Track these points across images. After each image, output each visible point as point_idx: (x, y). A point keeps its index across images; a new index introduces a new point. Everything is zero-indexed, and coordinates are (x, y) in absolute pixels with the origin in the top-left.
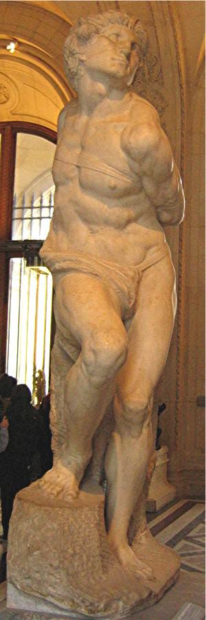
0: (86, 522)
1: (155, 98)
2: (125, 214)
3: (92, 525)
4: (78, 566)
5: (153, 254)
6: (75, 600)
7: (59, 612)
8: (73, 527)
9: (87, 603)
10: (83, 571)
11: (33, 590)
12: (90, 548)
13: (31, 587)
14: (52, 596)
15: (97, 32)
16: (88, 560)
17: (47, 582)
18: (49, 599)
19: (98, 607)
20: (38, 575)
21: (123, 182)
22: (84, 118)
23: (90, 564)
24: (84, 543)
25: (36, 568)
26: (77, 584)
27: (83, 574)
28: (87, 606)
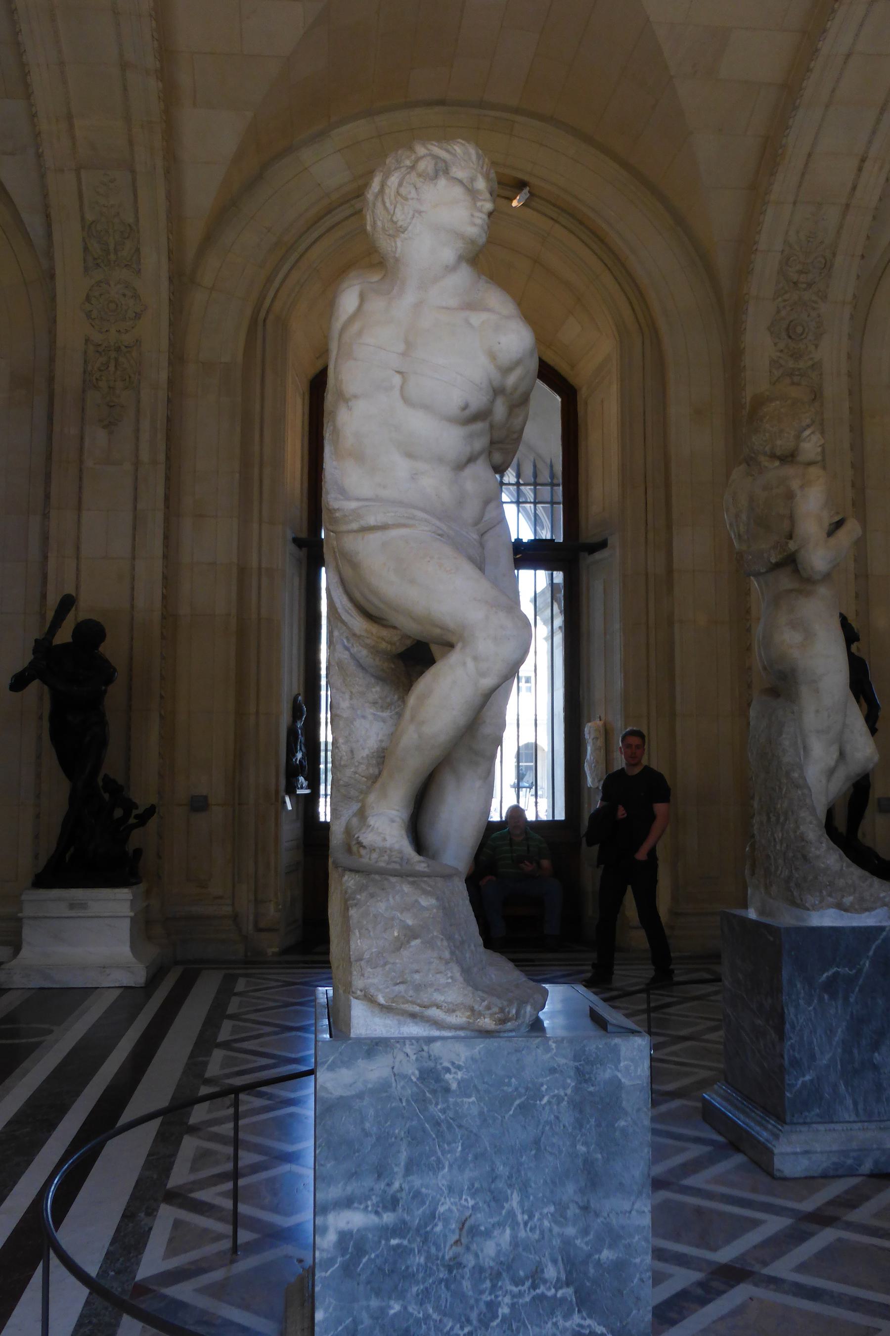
1: (124, 295)
6: (476, 1007)
7: (436, 1033)
9: (495, 1009)
11: (407, 1002)
13: (403, 997)
14: (438, 1007)
15: (446, 171)
17: (431, 985)
18: (434, 1012)
19: (509, 1012)
20: (417, 977)
21: (478, 401)
22: (409, 298)
25: (415, 967)
28: (491, 1015)
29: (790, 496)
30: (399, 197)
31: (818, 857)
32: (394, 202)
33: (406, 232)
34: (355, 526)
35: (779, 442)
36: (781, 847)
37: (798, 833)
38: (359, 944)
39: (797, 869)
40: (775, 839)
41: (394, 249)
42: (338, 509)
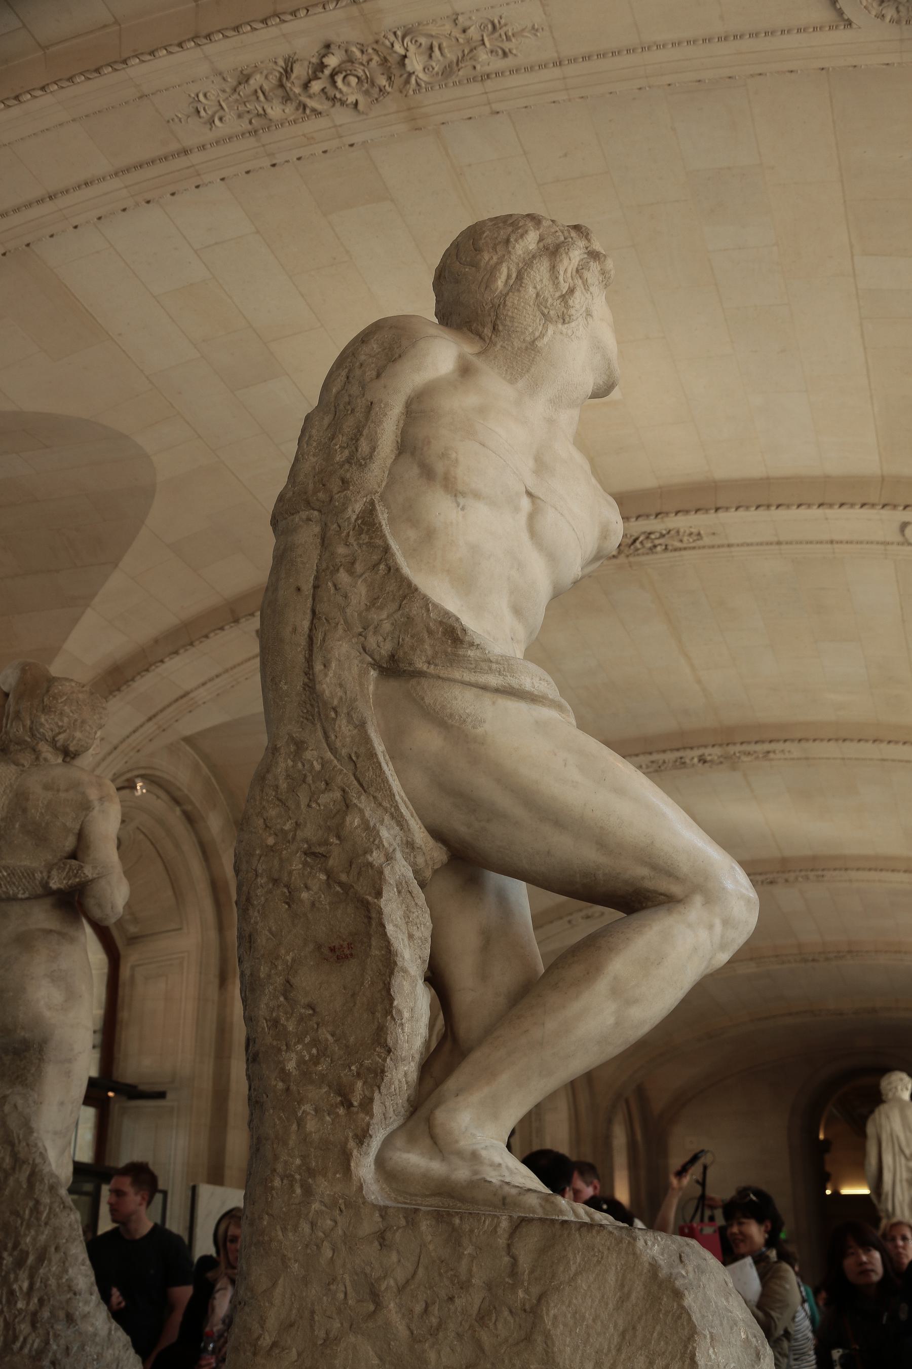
29: (86, 806)
30: (579, 279)
31: (85, 1316)
32: (570, 280)
33: (566, 326)
34: (493, 680)
35: (78, 734)
36: (28, 1304)
37: (64, 1280)
38: (713, 1357)
39: (56, 1336)
40: (12, 1293)
41: (537, 334)
42: (478, 645)
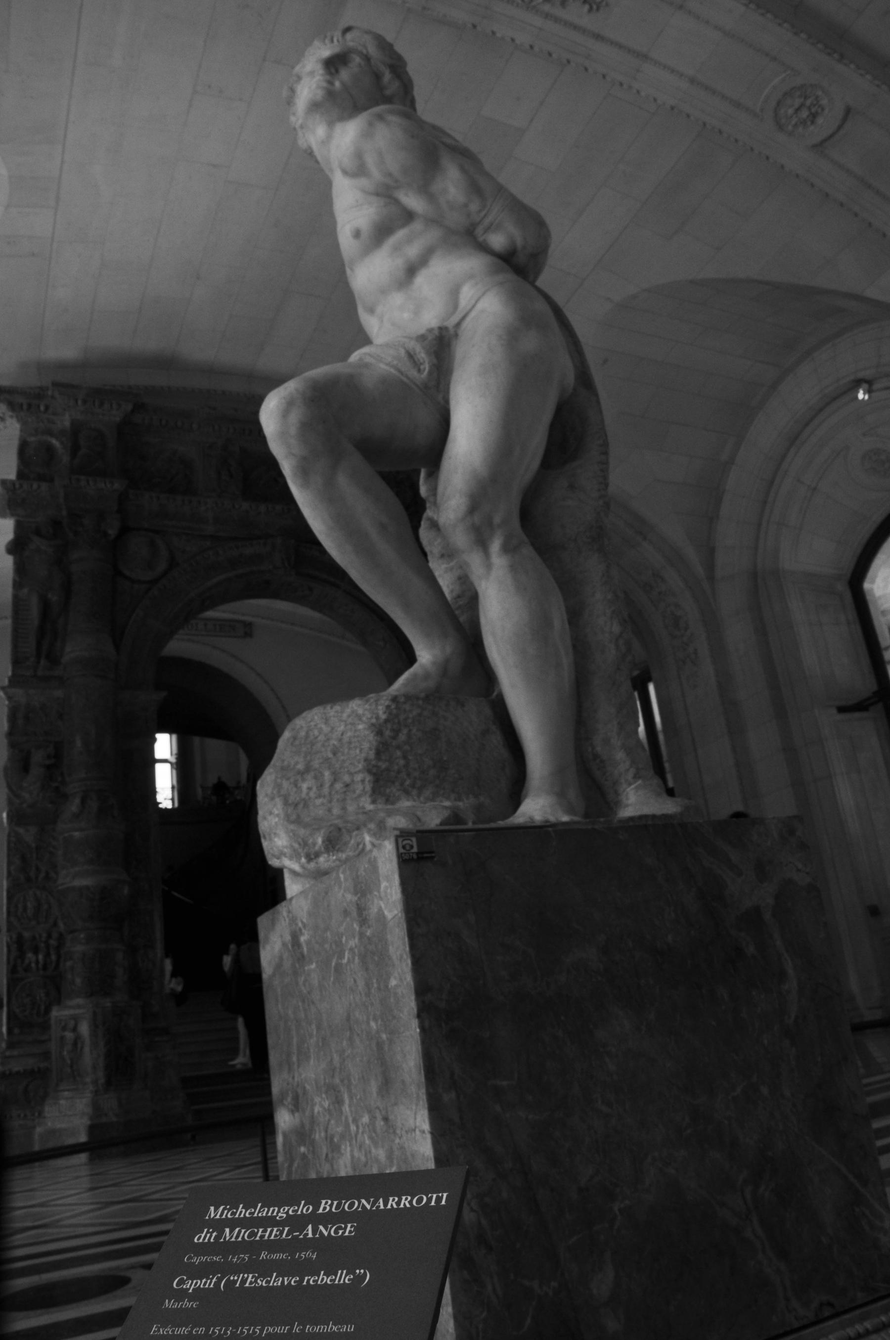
0: (350, 720)
2: (400, 262)
3: (361, 727)
4: (310, 789)
5: (467, 293)
8: (316, 732)
10: (319, 796)
12: (344, 761)
16: (335, 780)
19: (314, 844)
23: (338, 786)
24: (335, 754)
26: (298, 816)
27: (319, 802)
